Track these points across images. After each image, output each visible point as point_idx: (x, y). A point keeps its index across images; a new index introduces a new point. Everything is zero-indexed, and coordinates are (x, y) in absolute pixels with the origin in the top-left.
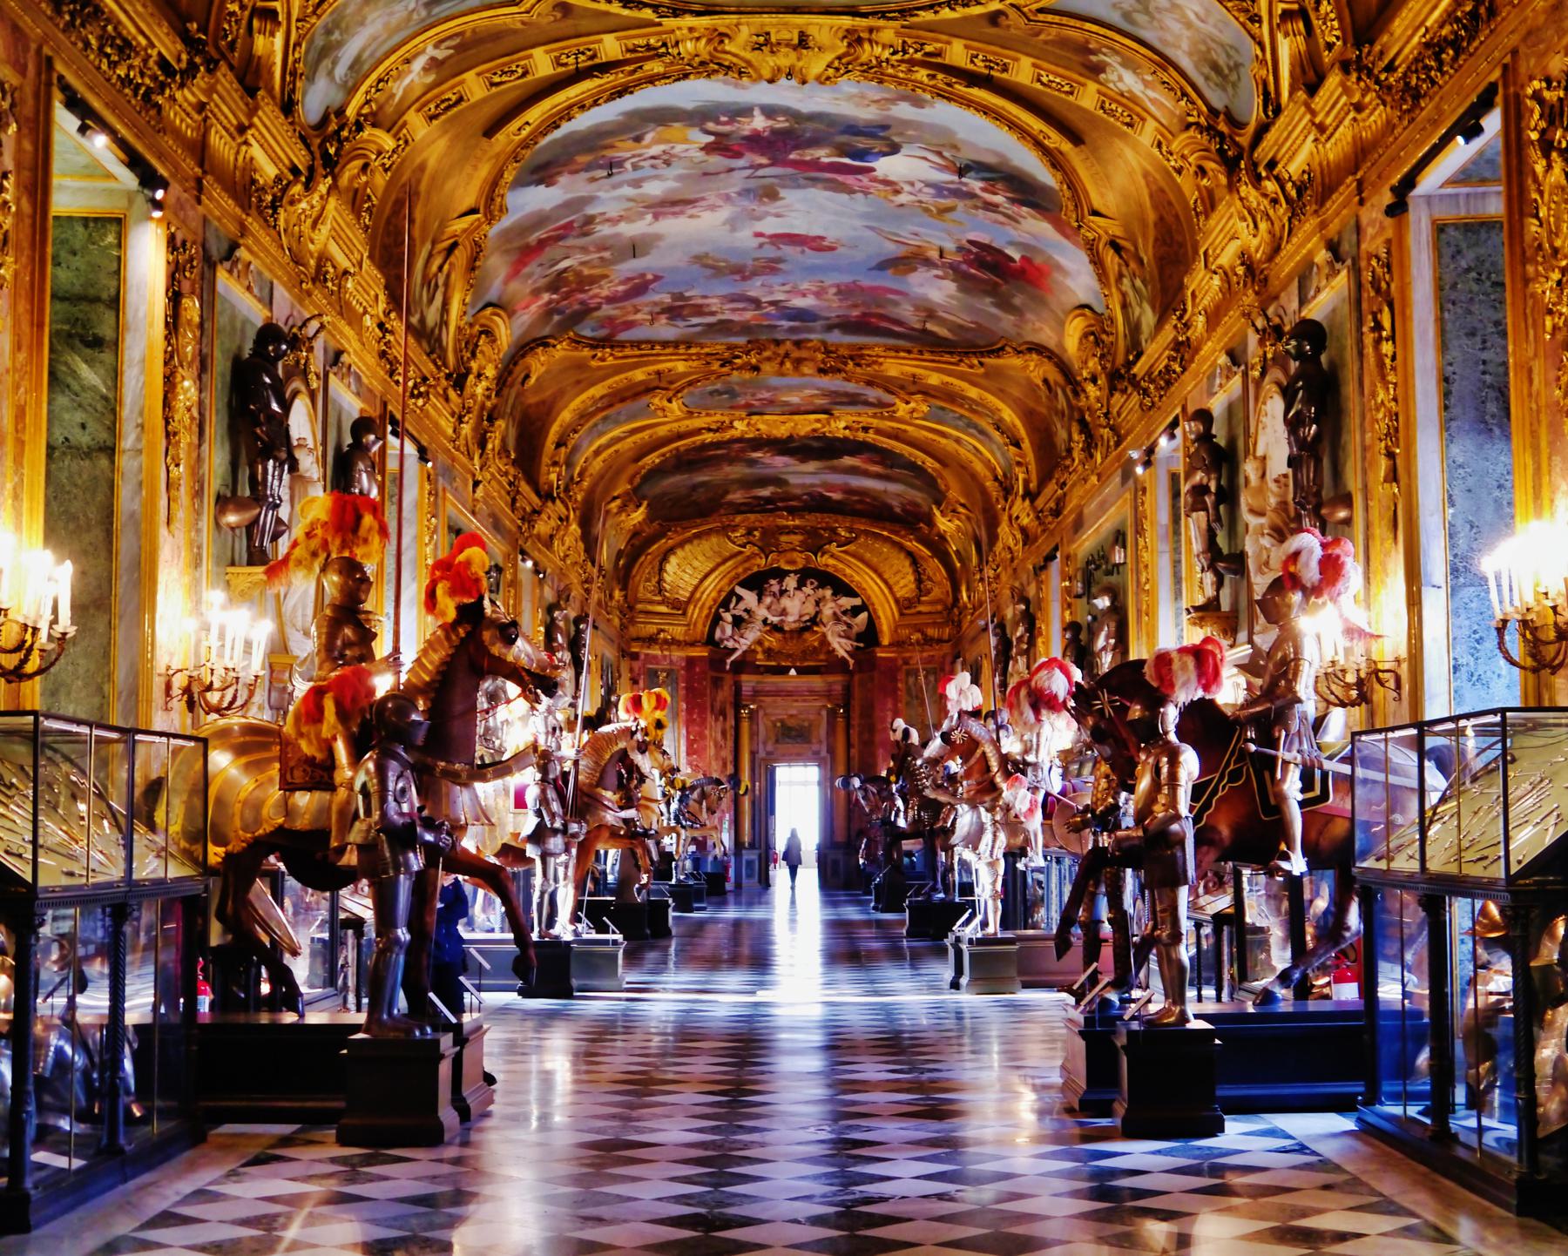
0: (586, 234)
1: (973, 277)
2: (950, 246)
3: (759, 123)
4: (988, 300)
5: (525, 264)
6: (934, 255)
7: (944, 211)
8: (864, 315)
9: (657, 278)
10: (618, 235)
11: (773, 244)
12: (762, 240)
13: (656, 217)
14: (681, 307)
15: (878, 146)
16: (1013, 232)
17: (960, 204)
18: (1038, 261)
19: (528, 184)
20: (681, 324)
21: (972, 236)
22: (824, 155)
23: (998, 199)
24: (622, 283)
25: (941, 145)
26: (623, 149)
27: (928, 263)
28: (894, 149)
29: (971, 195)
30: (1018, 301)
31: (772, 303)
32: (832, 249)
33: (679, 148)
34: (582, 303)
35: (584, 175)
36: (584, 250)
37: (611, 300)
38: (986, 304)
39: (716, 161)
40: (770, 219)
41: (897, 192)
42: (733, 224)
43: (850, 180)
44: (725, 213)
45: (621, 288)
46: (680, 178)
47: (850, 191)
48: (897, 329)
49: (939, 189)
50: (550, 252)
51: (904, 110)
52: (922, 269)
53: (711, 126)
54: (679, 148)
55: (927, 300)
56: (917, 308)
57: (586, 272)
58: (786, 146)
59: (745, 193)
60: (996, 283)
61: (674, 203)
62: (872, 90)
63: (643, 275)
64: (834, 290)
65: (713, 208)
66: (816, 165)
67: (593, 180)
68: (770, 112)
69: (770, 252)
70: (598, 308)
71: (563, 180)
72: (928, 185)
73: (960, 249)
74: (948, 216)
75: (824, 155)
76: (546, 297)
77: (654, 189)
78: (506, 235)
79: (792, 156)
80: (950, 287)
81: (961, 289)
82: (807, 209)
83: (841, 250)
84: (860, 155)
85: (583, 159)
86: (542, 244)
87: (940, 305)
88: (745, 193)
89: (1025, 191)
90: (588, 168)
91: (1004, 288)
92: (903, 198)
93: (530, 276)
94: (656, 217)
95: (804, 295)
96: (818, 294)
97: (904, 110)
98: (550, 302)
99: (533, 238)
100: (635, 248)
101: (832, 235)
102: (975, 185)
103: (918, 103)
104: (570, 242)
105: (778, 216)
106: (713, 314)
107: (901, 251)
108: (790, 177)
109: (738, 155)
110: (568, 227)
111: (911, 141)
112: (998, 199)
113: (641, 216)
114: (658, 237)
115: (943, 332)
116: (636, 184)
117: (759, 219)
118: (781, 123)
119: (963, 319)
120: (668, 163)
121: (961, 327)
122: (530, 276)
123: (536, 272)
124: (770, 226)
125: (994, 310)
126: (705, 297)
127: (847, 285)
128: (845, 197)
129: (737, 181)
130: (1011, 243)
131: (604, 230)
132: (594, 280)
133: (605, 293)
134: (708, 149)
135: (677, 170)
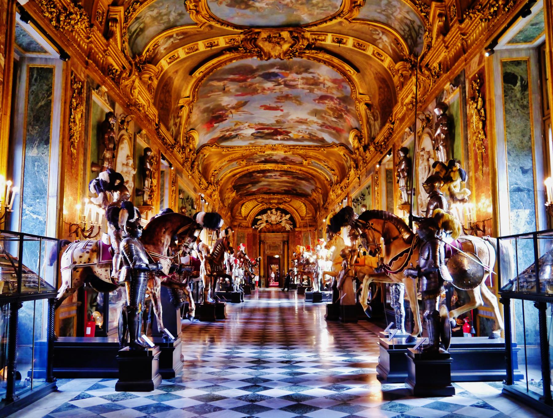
0: (324, 123)
1: (220, 111)
2: (230, 115)
3: (279, 137)
4: (211, 107)
5: (340, 129)
6: (233, 111)
7: (236, 124)
8: (245, 80)
9: (315, 100)
10: (318, 119)
11: (278, 107)
12: (281, 108)
13: (306, 120)
14: (312, 85)
15: (255, 134)
16: (218, 130)
17: (234, 128)
18: (211, 129)
19: (326, 142)
20: (315, 75)
21: (226, 121)
22: (266, 131)
23: (227, 133)
24: (325, 103)
25: (244, 138)
26: (307, 136)
27: (233, 108)
28: (252, 134)
29: (233, 131)
30: (206, 114)
31: (279, 84)
32: (261, 106)
33: (296, 133)
34: (340, 104)
35: (316, 135)
36: (327, 120)
37: (332, 99)
38: (211, 105)
39: (289, 130)
40: (278, 115)
41: (249, 126)
42: (288, 115)
43: (260, 127)
44: (289, 118)
45: (326, 102)
46: (297, 128)
47: (259, 124)
48: (231, 76)
49: (240, 129)
50: (334, 125)
51: (253, 142)
52: (234, 105)
53: (288, 137)
54: (296, 133)
55: (227, 96)
56: (229, 91)
57: (331, 113)
58: (275, 133)
59: (284, 122)
60: (213, 114)
61: (301, 122)
62: (258, 144)
63: (319, 103)
64: (259, 91)
65: (292, 119)
66: (268, 129)
67: (315, 133)
68: (277, 139)
69: (279, 105)
70: (338, 98)
71: (320, 137)
72: (242, 129)
73: (228, 116)
74: (235, 123)
75: (266, 131)
76: (345, 116)
77: (304, 127)
78: (337, 139)
79: (273, 131)
80: (224, 104)
81: (220, 105)
82: (269, 118)
83: (259, 106)
84: (259, 132)
85: (315, 138)
86: (334, 129)
87: (223, 96)
88: (284, 122)
89: (224, 138)
90: (315, 136)
91: (211, 115)
92: (247, 124)
93: (342, 126)
94: (306, 120)
95: (269, 88)
96: (264, 89)
97: (253, 142)
98: (346, 114)
99: (334, 132)
100: (315, 113)
101: (262, 111)
102: (233, 133)
103: (250, 143)
104: (329, 124)
105: (276, 116)
106: (303, 78)
107: (242, 109)
108: (273, 126)
109: (284, 131)
110: (326, 128)
111: (249, 137)
112: (227, 133)
113: (310, 121)
114: (309, 114)
115: (216, 83)
116: (307, 129)
117: (281, 116)
118: (275, 137)
119: (213, 95)
120: (299, 131)
121: (212, 92)
122: (342, 126)
123: (341, 125)
124: (279, 113)
125: (208, 105)
126: (303, 88)
127: (255, 94)
128: (261, 122)
129: (285, 126)
130: (218, 126)
131: (320, 122)
132: (332, 109)
133: (332, 103)
134: (290, 132)
135: (297, 129)
